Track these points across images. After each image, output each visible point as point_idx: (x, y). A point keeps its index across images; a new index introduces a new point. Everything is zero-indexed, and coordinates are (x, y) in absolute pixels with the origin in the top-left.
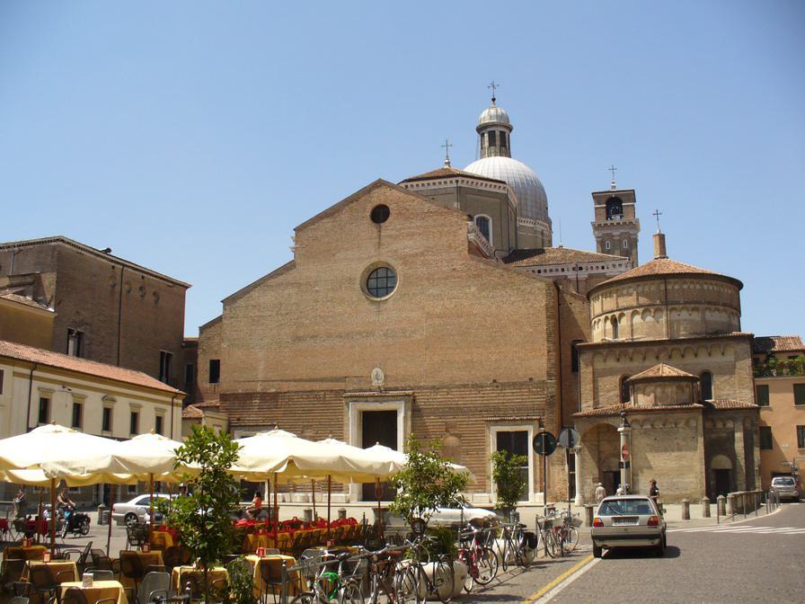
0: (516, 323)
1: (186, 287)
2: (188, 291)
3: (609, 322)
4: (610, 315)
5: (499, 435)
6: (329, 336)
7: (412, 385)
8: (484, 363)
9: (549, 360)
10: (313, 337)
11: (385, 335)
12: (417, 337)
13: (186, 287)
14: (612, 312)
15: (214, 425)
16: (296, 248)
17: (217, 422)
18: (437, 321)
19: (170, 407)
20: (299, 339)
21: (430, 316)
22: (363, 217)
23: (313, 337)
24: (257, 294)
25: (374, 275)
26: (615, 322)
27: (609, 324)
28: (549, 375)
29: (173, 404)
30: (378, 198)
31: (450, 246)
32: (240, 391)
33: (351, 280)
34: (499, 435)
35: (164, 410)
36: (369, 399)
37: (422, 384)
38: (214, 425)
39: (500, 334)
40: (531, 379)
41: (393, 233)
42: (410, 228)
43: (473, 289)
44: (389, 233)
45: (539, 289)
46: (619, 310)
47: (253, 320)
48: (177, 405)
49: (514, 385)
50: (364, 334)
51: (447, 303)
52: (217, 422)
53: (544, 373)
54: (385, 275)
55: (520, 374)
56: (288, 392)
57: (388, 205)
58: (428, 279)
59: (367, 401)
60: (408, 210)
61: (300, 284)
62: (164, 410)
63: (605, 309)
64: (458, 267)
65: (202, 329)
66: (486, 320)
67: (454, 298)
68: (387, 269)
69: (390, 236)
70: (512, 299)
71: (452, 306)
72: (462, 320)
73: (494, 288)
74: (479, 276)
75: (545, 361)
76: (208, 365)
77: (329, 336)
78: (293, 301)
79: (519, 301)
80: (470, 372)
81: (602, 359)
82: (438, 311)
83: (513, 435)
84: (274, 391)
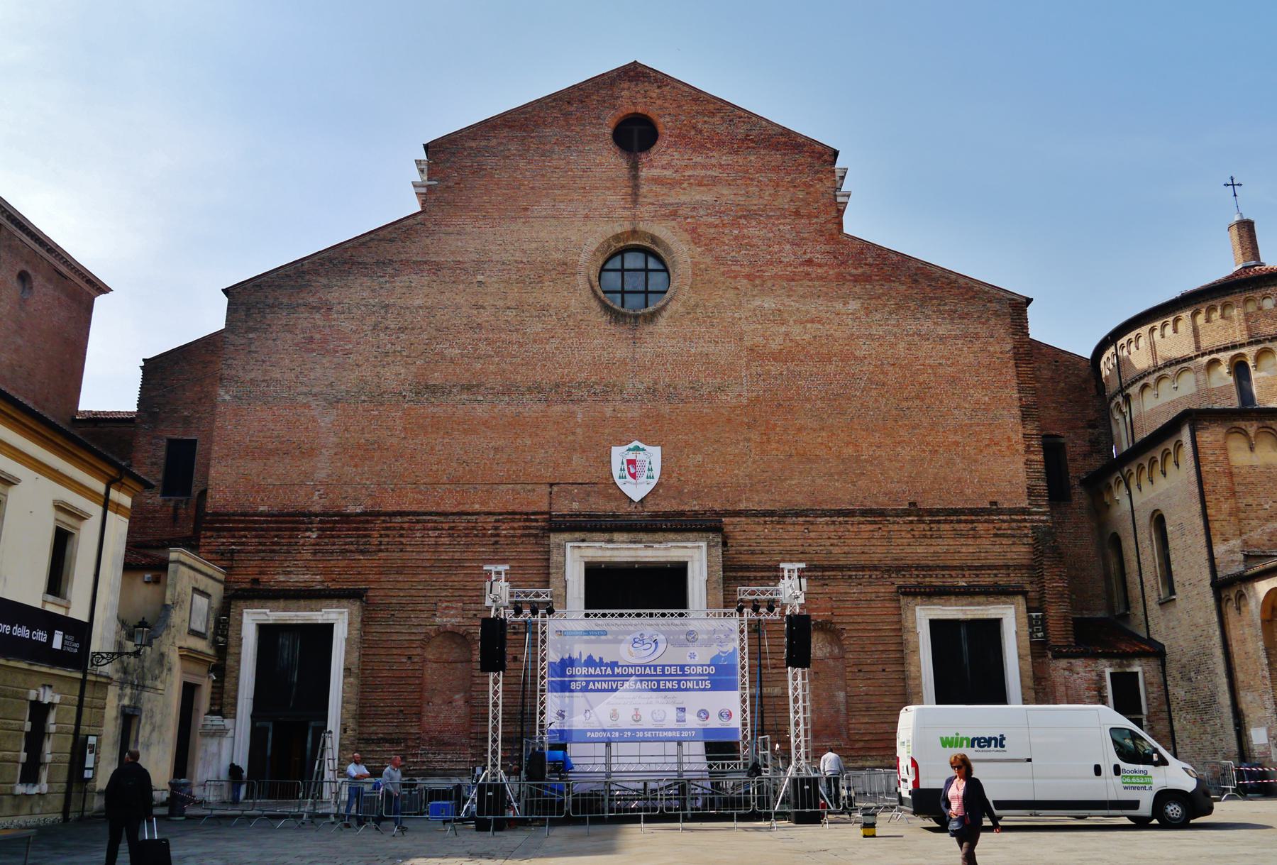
0: (953, 381)
1: (104, 289)
2: (100, 302)
3: (1224, 369)
4: (1225, 357)
5: (934, 624)
6: (509, 389)
7: (717, 507)
8: (887, 463)
9: (1028, 463)
10: (468, 388)
11: (652, 391)
12: (729, 398)
13: (104, 289)
14: (1234, 347)
15: (195, 590)
16: (428, 187)
17: (204, 583)
18: (774, 368)
19: (100, 509)
20: (433, 390)
21: (755, 353)
22: (596, 137)
23: (468, 388)
24: (324, 281)
25: (616, 263)
26: (1240, 369)
27: (1223, 376)
28: (1031, 492)
29: (106, 504)
30: (630, 101)
31: (797, 213)
32: (261, 509)
33: (566, 268)
34: (934, 624)
35: (81, 517)
36: (616, 536)
37: (742, 506)
38: (195, 590)
39: (917, 402)
40: (994, 503)
41: (668, 173)
42: (704, 167)
43: (854, 305)
44: (655, 172)
45: (996, 314)
46: (1258, 342)
47: (311, 340)
48: (118, 508)
49: (951, 513)
50: (598, 388)
51: (796, 330)
52: (204, 583)
53: (1023, 490)
54: (641, 265)
55: (968, 491)
56: (402, 514)
57: (655, 118)
58: (749, 277)
59: (610, 541)
60: (700, 131)
61: (438, 268)
62: (81, 517)
63: (1205, 344)
64: (819, 258)
65: (155, 370)
66: (885, 374)
67: (812, 321)
68: (647, 252)
69: (658, 181)
70: (941, 331)
71: (807, 337)
72: (831, 368)
73: (899, 307)
74: (867, 279)
75: (1021, 466)
76: (162, 453)
77: (509, 389)
78: (418, 302)
79: (956, 337)
80: (854, 483)
81: (1245, 446)
82: (774, 346)
83: (963, 632)
84: (358, 511)
